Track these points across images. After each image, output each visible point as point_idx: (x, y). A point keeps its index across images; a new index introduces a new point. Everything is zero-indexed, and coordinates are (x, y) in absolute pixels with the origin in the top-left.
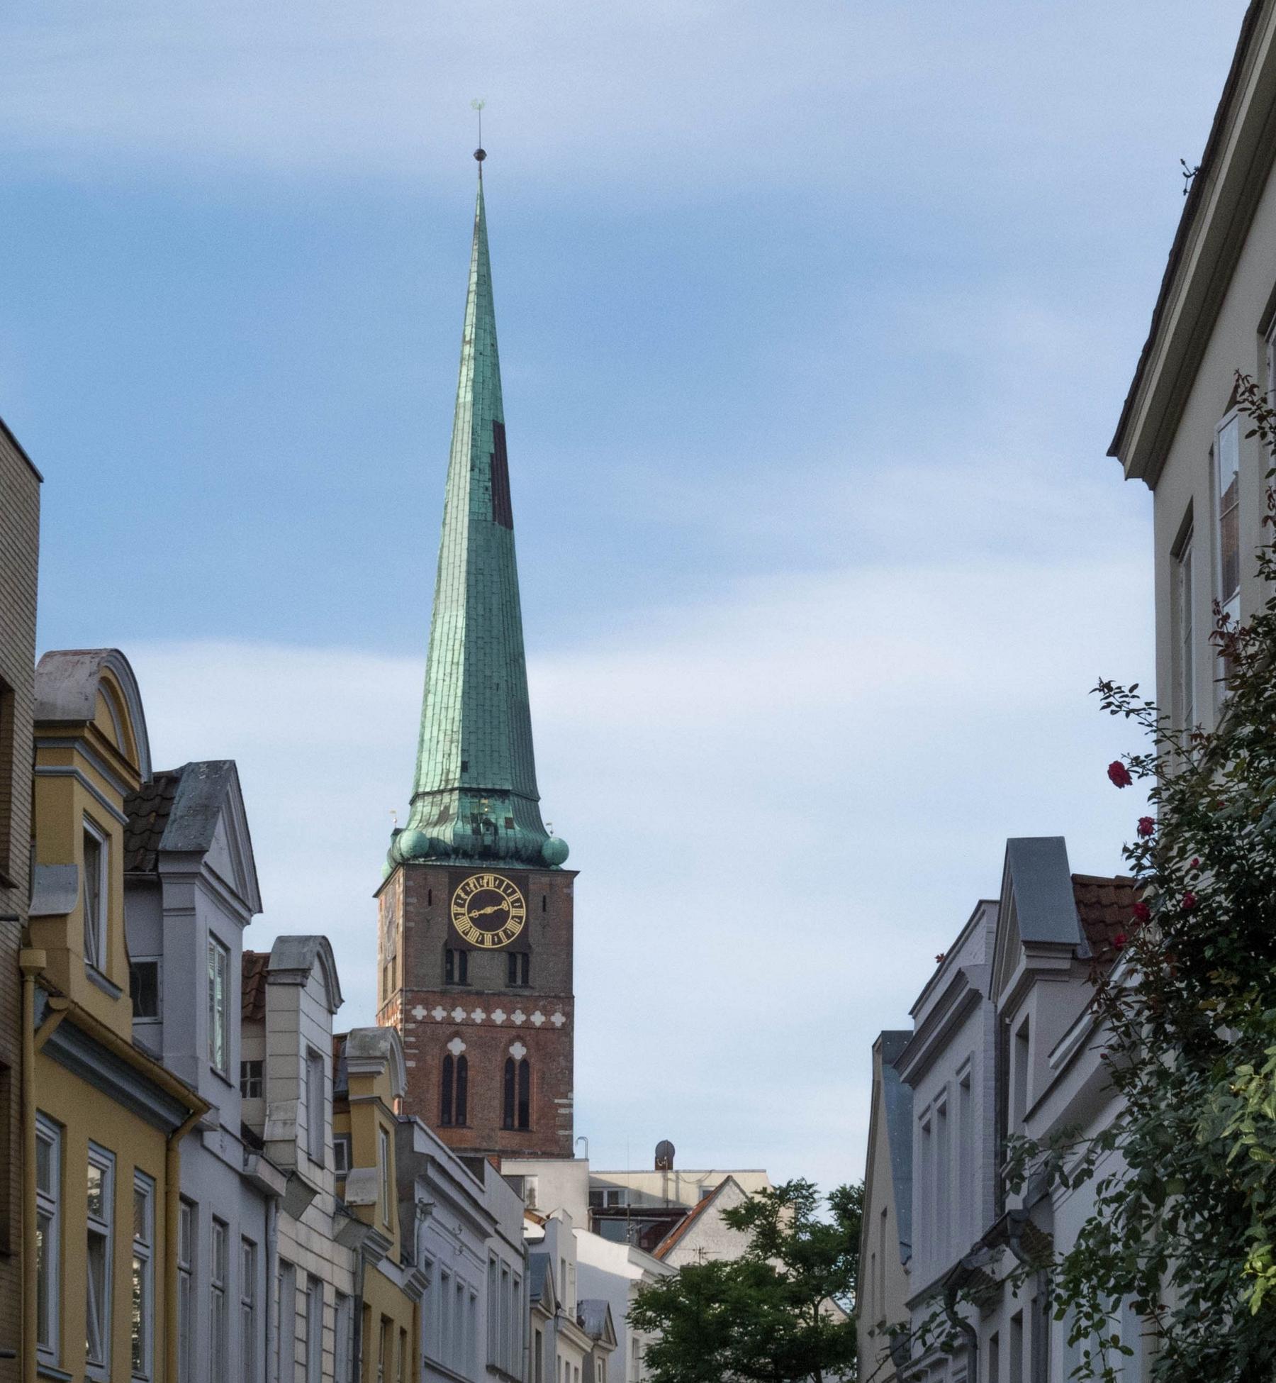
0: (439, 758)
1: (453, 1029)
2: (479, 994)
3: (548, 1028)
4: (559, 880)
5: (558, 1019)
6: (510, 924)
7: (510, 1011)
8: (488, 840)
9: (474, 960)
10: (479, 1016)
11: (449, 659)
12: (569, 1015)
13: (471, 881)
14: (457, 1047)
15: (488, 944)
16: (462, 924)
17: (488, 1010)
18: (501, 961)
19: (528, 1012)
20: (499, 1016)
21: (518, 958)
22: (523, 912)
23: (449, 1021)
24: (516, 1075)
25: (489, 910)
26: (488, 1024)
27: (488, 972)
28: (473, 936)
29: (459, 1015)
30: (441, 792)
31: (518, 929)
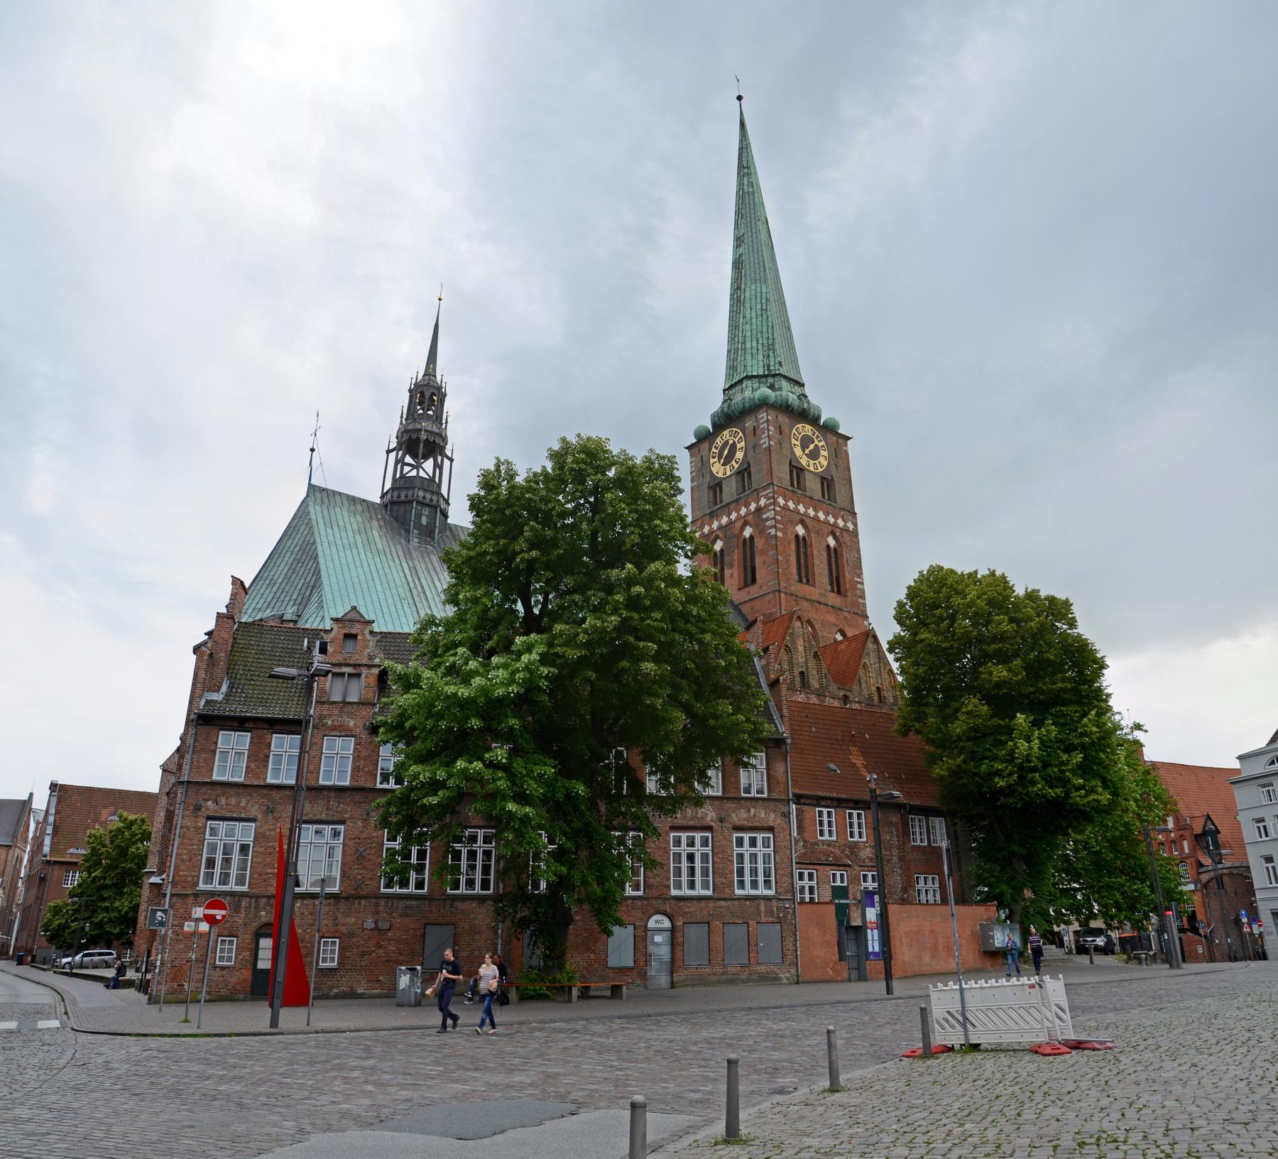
0: (761, 357)
1: (798, 517)
2: (811, 498)
3: (846, 530)
4: (841, 441)
5: (851, 526)
6: (821, 459)
7: (827, 514)
8: (806, 406)
9: (808, 476)
10: (811, 512)
11: (759, 306)
12: (855, 524)
13: (800, 426)
14: (800, 530)
15: (812, 468)
16: (798, 451)
17: (816, 510)
18: (818, 480)
19: (836, 518)
20: (821, 516)
21: (827, 482)
22: (826, 454)
23: (797, 511)
24: (834, 556)
25: (812, 447)
26: (816, 519)
27: (813, 486)
28: (804, 461)
29: (801, 508)
30: (765, 376)
31: (825, 463)
